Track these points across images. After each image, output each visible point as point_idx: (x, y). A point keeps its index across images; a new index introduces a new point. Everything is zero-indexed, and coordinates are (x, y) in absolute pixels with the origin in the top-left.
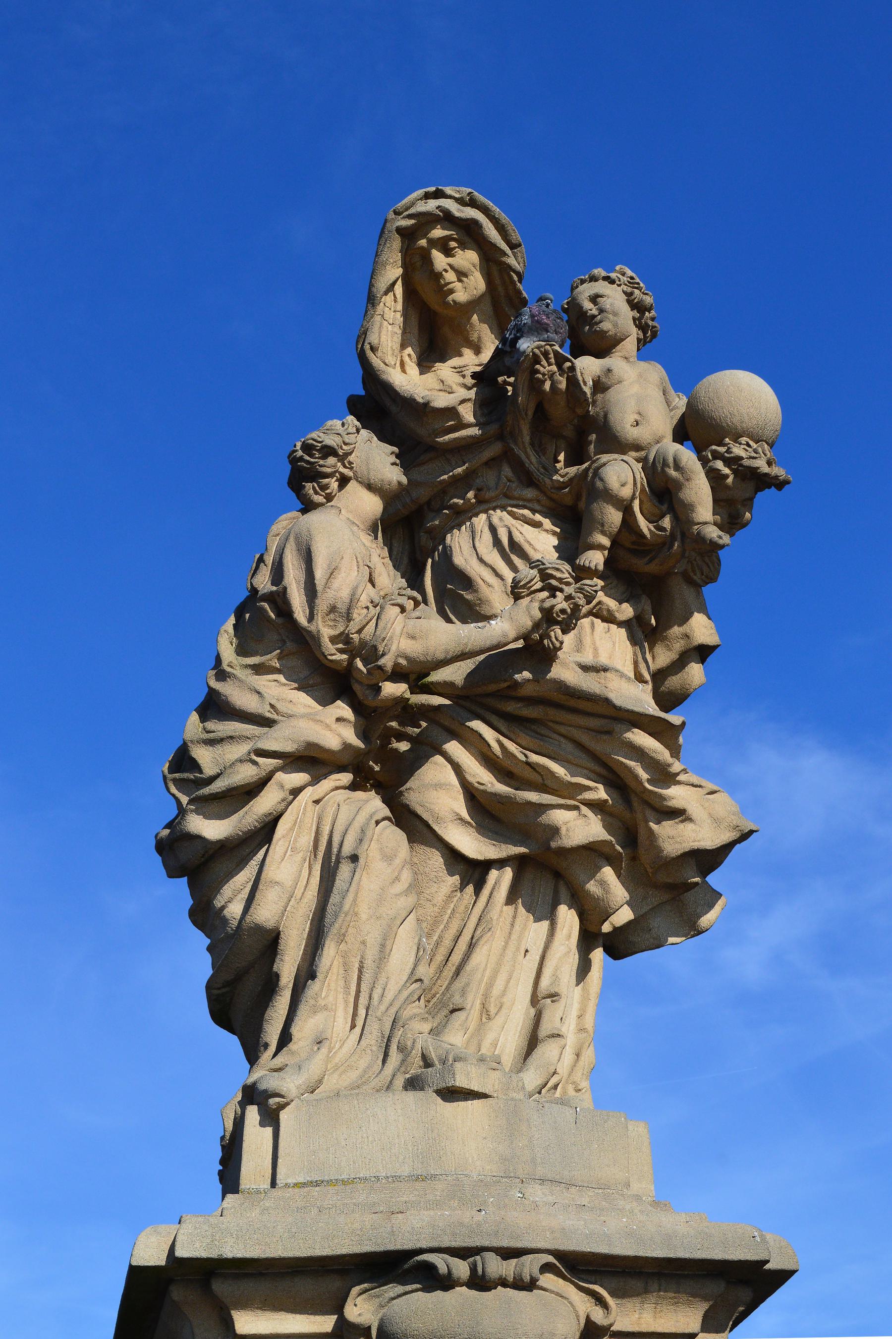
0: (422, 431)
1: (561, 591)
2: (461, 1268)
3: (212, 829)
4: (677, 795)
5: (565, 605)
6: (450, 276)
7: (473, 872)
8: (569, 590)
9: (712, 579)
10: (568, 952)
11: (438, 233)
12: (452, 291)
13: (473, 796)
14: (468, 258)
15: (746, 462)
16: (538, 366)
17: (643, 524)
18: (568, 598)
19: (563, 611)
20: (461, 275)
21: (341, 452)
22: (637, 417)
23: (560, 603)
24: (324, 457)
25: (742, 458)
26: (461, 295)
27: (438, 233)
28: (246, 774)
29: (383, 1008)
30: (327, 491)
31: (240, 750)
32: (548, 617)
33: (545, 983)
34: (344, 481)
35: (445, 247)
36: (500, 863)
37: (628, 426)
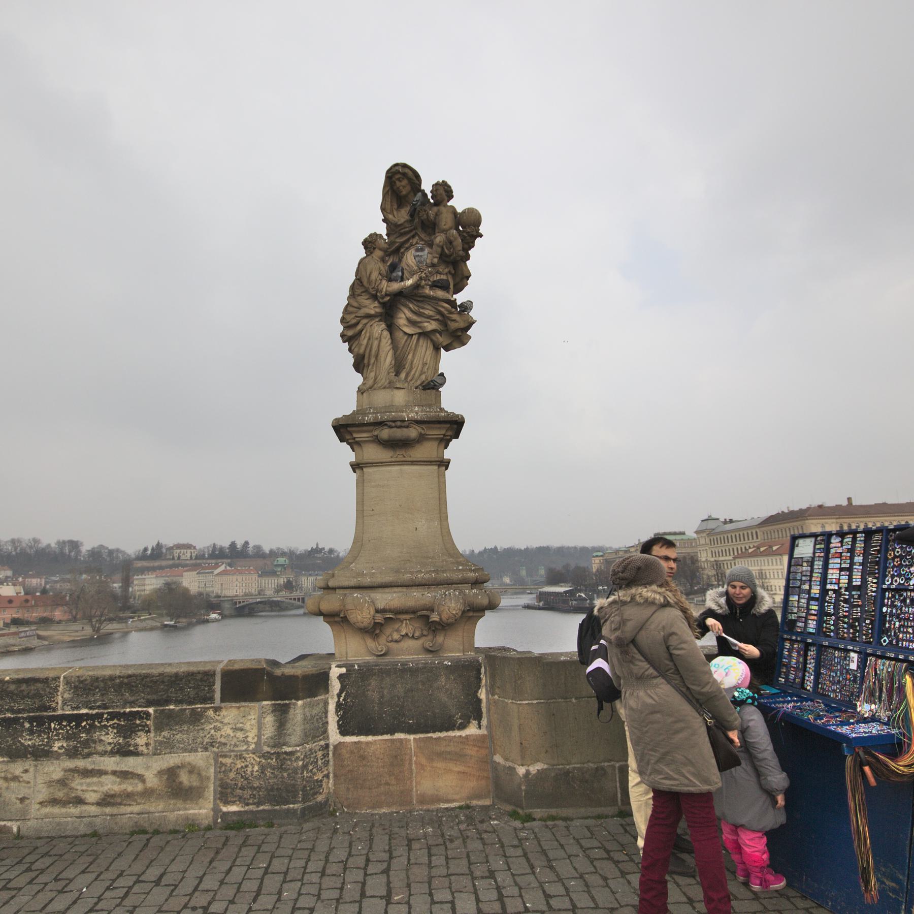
13: (409, 320)
14: (405, 182)
17: (446, 251)
23: (423, 275)
26: (404, 193)
28: (354, 321)
31: (353, 316)
32: (421, 278)
35: (399, 179)
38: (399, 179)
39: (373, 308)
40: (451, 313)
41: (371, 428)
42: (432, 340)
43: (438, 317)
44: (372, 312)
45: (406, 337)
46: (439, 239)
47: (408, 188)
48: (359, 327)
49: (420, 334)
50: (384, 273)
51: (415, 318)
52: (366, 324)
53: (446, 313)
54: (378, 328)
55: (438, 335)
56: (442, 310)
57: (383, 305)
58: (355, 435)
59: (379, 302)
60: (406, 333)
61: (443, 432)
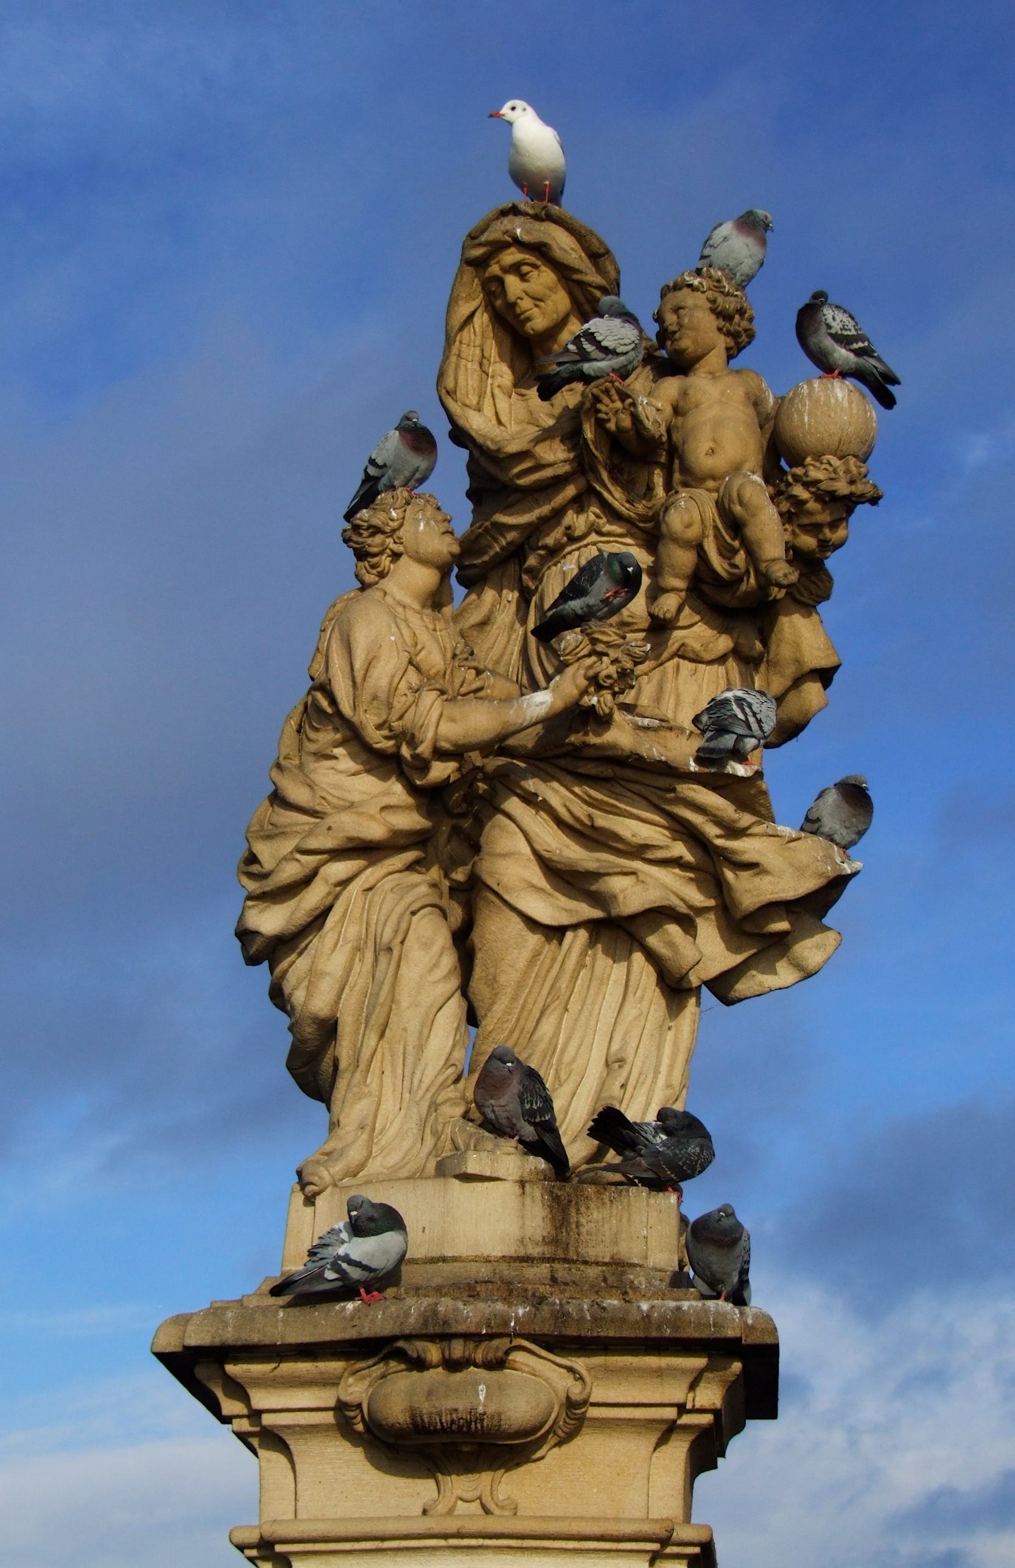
0: (501, 476)
1: (607, 655)
2: (433, 1353)
3: (270, 921)
4: (747, 848)
5: (612, 670)
6: (526, 304)
7: (555, 933)
8: (613, 653)
9: (827, 597)
10: (640, 1015)
11: (511, 256)
12: (529, 319)
14: (544, 278)
15: (822, 486)
16: (599, 406)
18: (615, 661)
19: (609, 677)
20: (537, 299)
21: (388, 529)
22: (711, 444)
23: (606, 668)
24: (372, 535)
25: (820, 481)
26: (539, 322)
27: (511, 256)
28: (290, 872)
29: (421, 1093)
30: (379, 569)
31: (287, 846)
32: (595, 682)
33: (615, 1047)
34: (396, 556)
36: (575, 927)
37: (702, 456)
38: (515, 269)
39: (376, 804)
40: (734, 832)
41: (334, 1366)
42: (651, 956)
43: (679, 849)
44: (375, 831)
45: (534, 940)
46: (690, 513)
47: (560, 301)
48: (313, 897)
49: (594, 927)
50: (434, 658)
51: (572, 852)
52: (345, 883)
53: (711, 831)
54: (394, 899)
55: (673, 929)
56: (696, 819)
57: (430, 798)
58: (260, 1399)
59: (412, 789)
60: (532, 924)
61: (677, 1393)
